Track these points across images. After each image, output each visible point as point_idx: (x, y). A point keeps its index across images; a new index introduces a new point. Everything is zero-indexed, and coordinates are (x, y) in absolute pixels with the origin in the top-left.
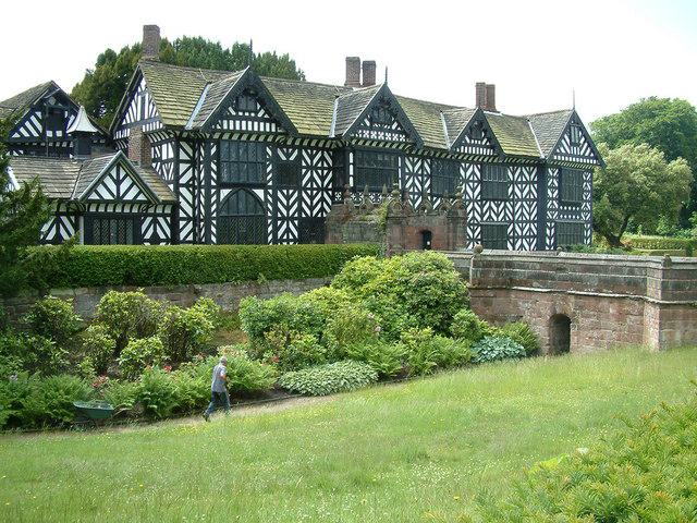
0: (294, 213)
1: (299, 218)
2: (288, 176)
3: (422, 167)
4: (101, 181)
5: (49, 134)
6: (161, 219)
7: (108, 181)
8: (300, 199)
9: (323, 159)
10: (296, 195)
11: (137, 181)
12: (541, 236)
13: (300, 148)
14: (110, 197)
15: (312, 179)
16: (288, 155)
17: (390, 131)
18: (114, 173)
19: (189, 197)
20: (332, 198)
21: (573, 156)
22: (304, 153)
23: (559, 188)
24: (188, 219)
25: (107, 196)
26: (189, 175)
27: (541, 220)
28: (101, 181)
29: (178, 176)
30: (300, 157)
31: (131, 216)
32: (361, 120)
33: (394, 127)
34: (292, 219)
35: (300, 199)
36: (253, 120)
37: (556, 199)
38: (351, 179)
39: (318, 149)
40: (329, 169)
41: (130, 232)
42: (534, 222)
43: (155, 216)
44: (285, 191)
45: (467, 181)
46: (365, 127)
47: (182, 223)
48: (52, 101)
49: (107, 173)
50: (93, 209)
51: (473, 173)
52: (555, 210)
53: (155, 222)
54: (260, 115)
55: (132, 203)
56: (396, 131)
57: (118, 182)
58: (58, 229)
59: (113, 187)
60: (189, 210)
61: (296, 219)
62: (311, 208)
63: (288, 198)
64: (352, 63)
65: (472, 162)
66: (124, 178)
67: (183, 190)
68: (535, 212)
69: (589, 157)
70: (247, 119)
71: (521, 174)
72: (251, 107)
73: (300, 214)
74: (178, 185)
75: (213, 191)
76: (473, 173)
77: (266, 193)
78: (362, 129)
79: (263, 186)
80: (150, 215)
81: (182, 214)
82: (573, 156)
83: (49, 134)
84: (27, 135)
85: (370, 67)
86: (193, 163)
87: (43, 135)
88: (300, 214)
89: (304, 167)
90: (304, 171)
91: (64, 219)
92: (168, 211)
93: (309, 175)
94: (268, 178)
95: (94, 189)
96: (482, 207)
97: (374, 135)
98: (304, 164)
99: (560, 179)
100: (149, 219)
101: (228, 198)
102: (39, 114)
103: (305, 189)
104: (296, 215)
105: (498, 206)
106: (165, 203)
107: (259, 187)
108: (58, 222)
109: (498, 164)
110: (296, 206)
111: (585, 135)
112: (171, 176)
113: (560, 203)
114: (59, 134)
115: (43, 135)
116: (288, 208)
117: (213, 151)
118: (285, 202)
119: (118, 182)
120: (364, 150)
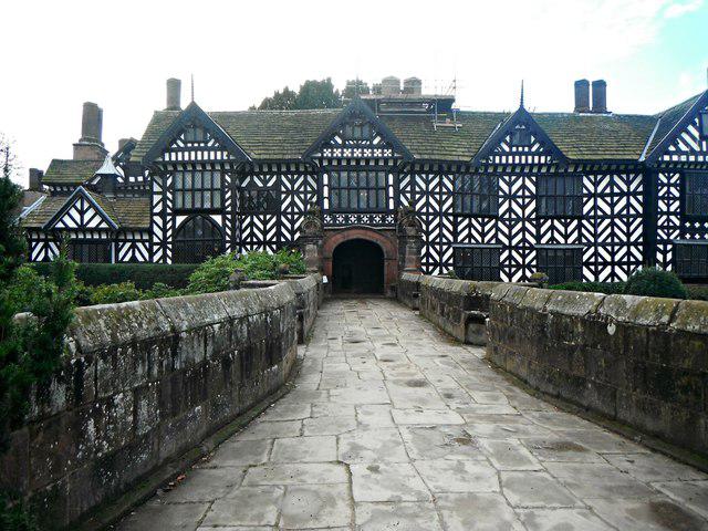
0: (272, 237)
3: (441, 184)
6: (140, 245)
8: (279, 224)
9: (305, 183)
10: (274, 220)
11: (98, 212)
13: (279, 173)
14: (75, 226)
15: (293, 204)
16: (265, 182)
17: (371, 147)
18: (78, 205)
22: (283, 178)
25: (72, 225)
27: (649, 244)
30: (279, 183)
31: (100, 241)
33: (376, 142)
35: (279, 224)
36: (202, 150)
37: (675, 213)
39: (300, 174)
41: (101, 254)
42: (636, 244)
44: (262, 217)
45: (511, 197)
51: (524, 187)
52: (675, 227)
53: (134, 247)
54: (210, 144)
55: (97, 230)
56: (377, 147)
57: (82, 213)
58: (134, 252)
59: (77, 216)
61: (274, 243)
63: (265, 223)
64: (581, 86)
65: (522, 174)
66: (87, 210)
68: (640, 230)
70: (196, 150)
71: (612, 184)
72: (200, 136)
73: (279, 239)
75: (169, 218)
76: (524, 187)
77: (224, 219)
78: (332, 147)
79: (221, 211)
80: (129, 241)
85: (600, 86)
88: (279, 239)
89: (284, 192)
90: (283, 196)
93: (289, 199)
94: (227, 204)
96: (538, 227)
97: (347, 153)
98: (283, 189)
99: (681, 186)
100: (128, 245)
101: (183, 224)
103: (285, 213)
104: (274, 240)
105: (566, 226)
106: (141, 231)
107: (216, 212)
108: (46, 247)
109: (562, 175)
110: (274, 230)
113: (683, 221)
114: (140, 179)
116: (265, 233)
117: (169, 182)
118: (261, 227)
119: (82, 213)
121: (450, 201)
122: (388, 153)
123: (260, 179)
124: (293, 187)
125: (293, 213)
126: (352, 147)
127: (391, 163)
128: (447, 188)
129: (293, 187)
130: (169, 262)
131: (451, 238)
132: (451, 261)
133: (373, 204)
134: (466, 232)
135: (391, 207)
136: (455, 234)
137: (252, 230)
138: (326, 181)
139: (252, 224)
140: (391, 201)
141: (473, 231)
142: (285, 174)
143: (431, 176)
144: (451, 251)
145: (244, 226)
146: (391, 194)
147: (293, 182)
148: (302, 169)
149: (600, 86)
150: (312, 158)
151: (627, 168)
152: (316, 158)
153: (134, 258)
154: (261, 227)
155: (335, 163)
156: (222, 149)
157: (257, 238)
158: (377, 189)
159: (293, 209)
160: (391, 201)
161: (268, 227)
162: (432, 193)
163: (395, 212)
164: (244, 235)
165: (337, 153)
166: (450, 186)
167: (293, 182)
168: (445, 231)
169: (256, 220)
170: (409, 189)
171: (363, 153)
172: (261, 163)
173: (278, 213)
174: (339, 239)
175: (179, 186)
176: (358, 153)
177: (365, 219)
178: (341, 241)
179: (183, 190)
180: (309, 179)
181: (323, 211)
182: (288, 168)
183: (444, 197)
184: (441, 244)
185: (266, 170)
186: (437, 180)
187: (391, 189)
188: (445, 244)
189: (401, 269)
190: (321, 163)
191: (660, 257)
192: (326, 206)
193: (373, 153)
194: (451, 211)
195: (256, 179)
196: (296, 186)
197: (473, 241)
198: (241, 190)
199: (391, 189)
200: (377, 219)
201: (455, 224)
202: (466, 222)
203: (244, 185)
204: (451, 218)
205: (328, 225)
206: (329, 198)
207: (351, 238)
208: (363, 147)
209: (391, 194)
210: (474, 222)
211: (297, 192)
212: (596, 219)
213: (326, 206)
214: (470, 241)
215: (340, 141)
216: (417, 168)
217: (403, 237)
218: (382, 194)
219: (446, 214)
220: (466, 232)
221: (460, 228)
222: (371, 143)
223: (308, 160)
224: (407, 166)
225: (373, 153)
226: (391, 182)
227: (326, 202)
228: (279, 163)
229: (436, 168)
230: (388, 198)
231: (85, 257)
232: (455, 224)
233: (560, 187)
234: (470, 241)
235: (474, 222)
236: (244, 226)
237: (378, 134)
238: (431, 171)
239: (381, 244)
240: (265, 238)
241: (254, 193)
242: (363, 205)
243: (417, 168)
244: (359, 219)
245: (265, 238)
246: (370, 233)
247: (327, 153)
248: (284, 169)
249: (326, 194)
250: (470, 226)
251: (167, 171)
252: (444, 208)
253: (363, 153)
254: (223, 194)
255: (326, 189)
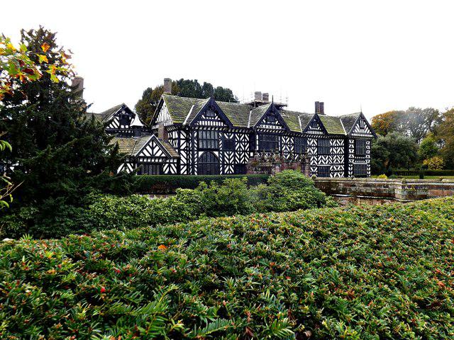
1: (235, 164)
2: (229, 146)
4: (145, 148)
5: (122, 127)
6: (172, 165)
7: (148, 148)
8: (235, 156)
9: (245, 138)
11: (161, 148)
12: (346, 171)
13: (235, 133)
15: (240, 147)
16: (229, 136)
17: (274, 125)
18: (151, 144)
19: (185, 155)
20: (249, 155)
21: (361, 133)
23: (355, 149)
24: (185, 165)
25: (148, 155)
26: (185, 145)
27: (346, 164)
28: (145, 148)
29: (179, 146)
30: (235, 137)
31: (158, 163)
32: (262, 120)
33: (277, 123)
34: (231, 164)
35: (235, 156)
36: (213, 121)
38: (257, 147)
39: (243, 134)
40: (248, 142)
43: (170, 163)
45: (310, 147)
46: (263, 124)
47: (182, 167)
48: (124, 112)
49: (148, 144)
50: (141, 160)
51: (314, 143)
53: (169, 166)
54: (216, 118)
55: (159, 158)
56: (277, 125)
60: (185, 161)
62: (240, 160)
63: (229, 155)
65: (313, 138)
67: (182, 152)
69: (369, 134)
70: (210, 120)
71: (336, 142)
74: (180, 150)
76: (314, 143)
77: (219, 153)
81: (182, 163)
82: (361, 133)
83: (122, 127)
84: (112, 127)
86: (187, 140)
87: (119, 127)
91: (128, 165)
92: (175, 161)
95: (142, 151)
96: (318, 158)
97: (267, 127)
99: (355, 144)
100: (167, 165)
102: (118, 118)
106: (174, 158)
111: (367, 124)
112: (177, 146)
114: (127, 127)
115: (119, 127)
116: (229, 160)
117: (195, 135)
120: (263, 133)
122: (280, 128)
125: (240, 151)
130: (196, 173)
147: (240, 137)
149: (322, 104)
151: (342, 137)
153: (170, 172)
156: (221, 121)
167: (240, 137)
175: (200, 137)
179: (203, 139)
191: (349, 169)
212: (333, 155)
231: (150, 172)
233: (324, 144)
251: (194, 129)
254: (219, 141)
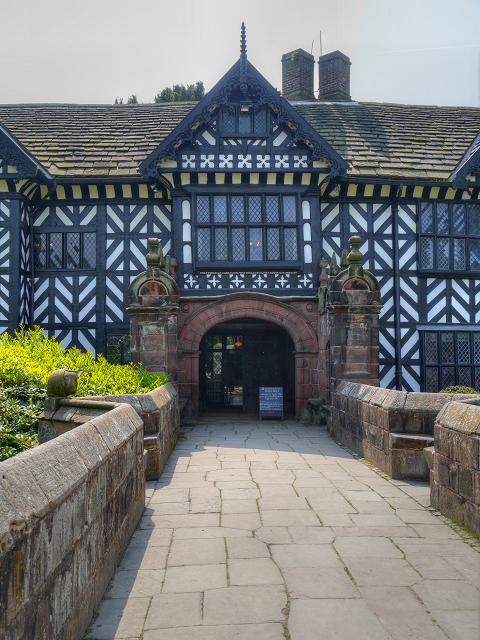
0: (89, 316)
1: (100, 325)
3: (394, 220)
8: (101, 292)
9: (150, 219)
13: (102, 202)
15: (127, 256)
16: (77, 217)
17: (270, 151)
22: (110, 211)
33: (278, 142)
35: (101, 292)
39: (140, 203)
44: (70, 280)
46: (208, 150)
56: (282, 151)
61: (92, 326)
63: (75, 290)
73: (101, 319)
78: (198, 151)
88: (101, 319)
90: (110, 242)
93: (120, 248)
97: (226, 162)
104: (93, 319)
116: (76, 307)
118: (69, 297)
121: (411, 251)
122: (301, 162)
123: (67, 212)
124: (127, 226)
126: (235, 152)
127: (306, 180)
128: (405, 227)
129: (127, 226)
131: (415, 315)
132: (416, 356)
133: (274, 255)
134: (442, 303)
135: (308, 257)
136: (422, 307)
137: (52, 302)
138: (186, 215)
139: (52, 293)
140: (308, 250)
141: (455, 303)
142: (113, 203)
143: (376, 207)
144: (414, 339)
145: (37, 295)
146: (307, 235)
147: (127, 218)
148: (143, 193)
150: (161, 171)
152: (168, 171)
154: (69, 297)
155: (203, 179)
157: (61, 316)
158: (282, 226)
159: (127, 266)
160: (308, 250)
161: (82, 297)
162: (380, 237)
163: (316, 268)
164: (37, 313)
165: (208, 161)
166: (412, 225)
167: (127, 218)
168: (404, 303)
169: (59, 285)
170: (337, 229)
171: (254, 161)
172: (68, 183)
173: (101, 272)
174: (210, 317)
176: (245, 162)
177: (260, 281)
178: (216, 320)
180: (157, 211)
181: (179, 268)
182: (119, 192)
183: (401, 243)
184: (396, 325)
185: (77, 194)
186: (387, 214)
187: (307, 228)
188: (404, 325)
189: (337, 373)
190: (177, 179)
192: (187, 257)
193: (272, 161)
194: (413, 267)
195: (59, 212)
196: (133, 225)
197: (455, 320)
198: (29, 230)
199: (307, 228)
200: (282, 281)
201: (422, 291)
202: (442, 286)
203: (38, 223)
204: (415, 280)
205: (192, 291)
206: (193, 244)
207: (233, 315)
208: (255, 152)
209: (307, 235)
210: (455, 286)
211: (136, 236)
213: (187, 257)
214: (449, 319)
215: (212, 141)
216: (352, 191)
217: (341, 311)
218: (291, 234)
219: (405, 273)
220: (442, 303)
221: (430, 297)
222: (270, 143)
223: (151, 173)
224: (335, 188)
225: (272, 161)
226: (306, 215)
227: (187, 252)
228: (101, 185)
229: (385, 192)
230: (301, 243)
232: (422, 291)
234: (449, 319)
235: (455, 286)
236: (37, 295)
237: (283, 127)
238: (376, 198)
239: (285, 324)
240: (75, 317)
241: (56, 238)
242: (256, 256)
243: (352, 191)
244: (249, 281)
245: (75, 317)
246: (267, 307)
247: (189, 162)
248: (111, 193)
249: (187, 236)
250: (449, 293)
252: (402, 262)
253: (254, 161)
255: (187, 229)
